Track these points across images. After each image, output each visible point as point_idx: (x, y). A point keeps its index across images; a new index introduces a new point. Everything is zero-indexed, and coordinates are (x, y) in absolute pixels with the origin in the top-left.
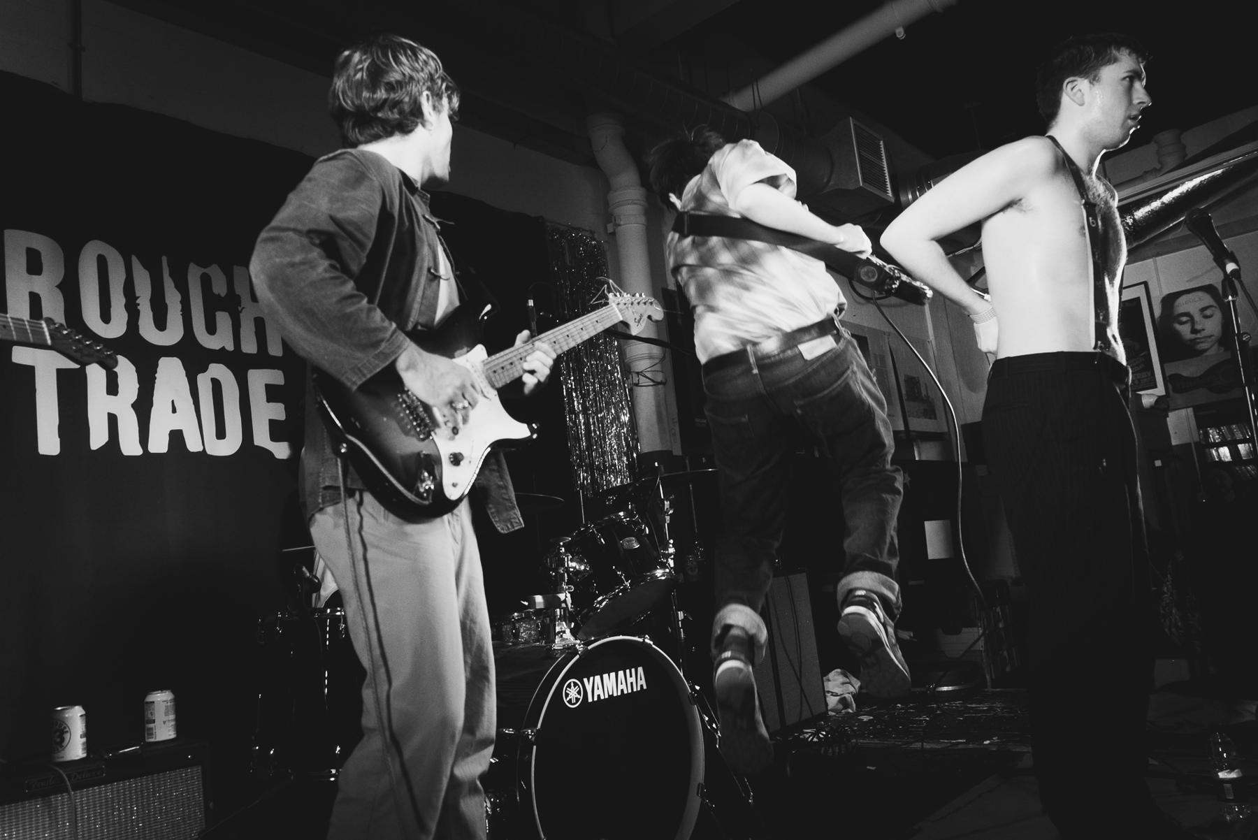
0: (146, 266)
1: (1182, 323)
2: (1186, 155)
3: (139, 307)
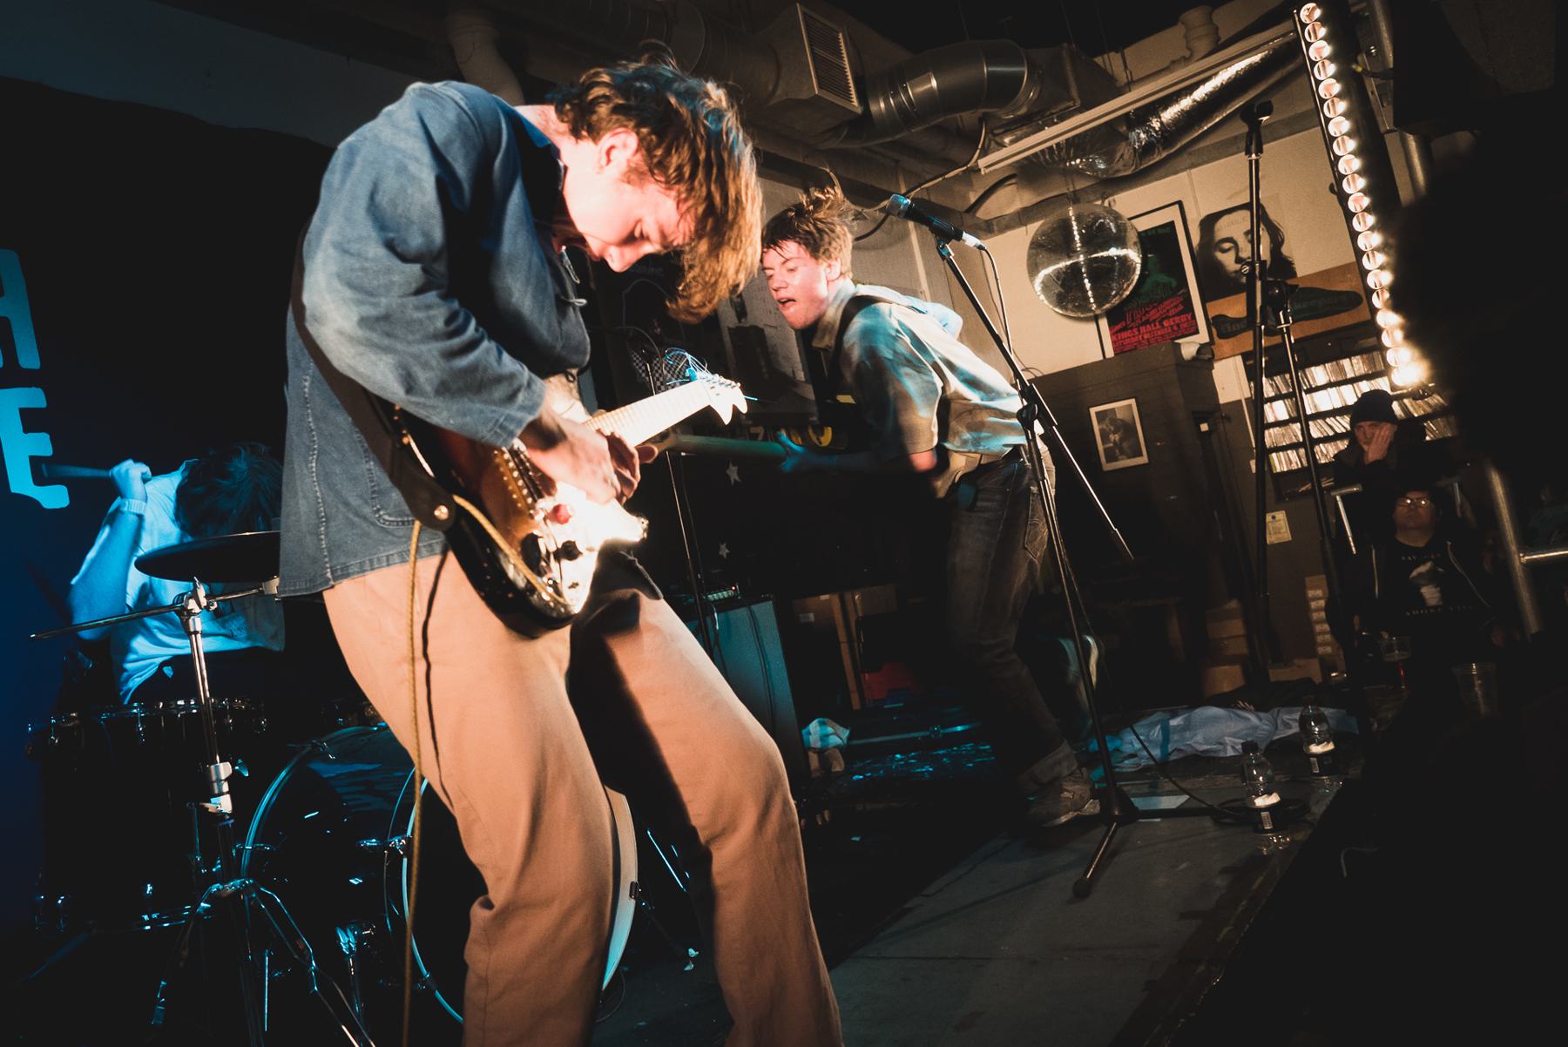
1: (1224, 251)
2: (1219, 39)
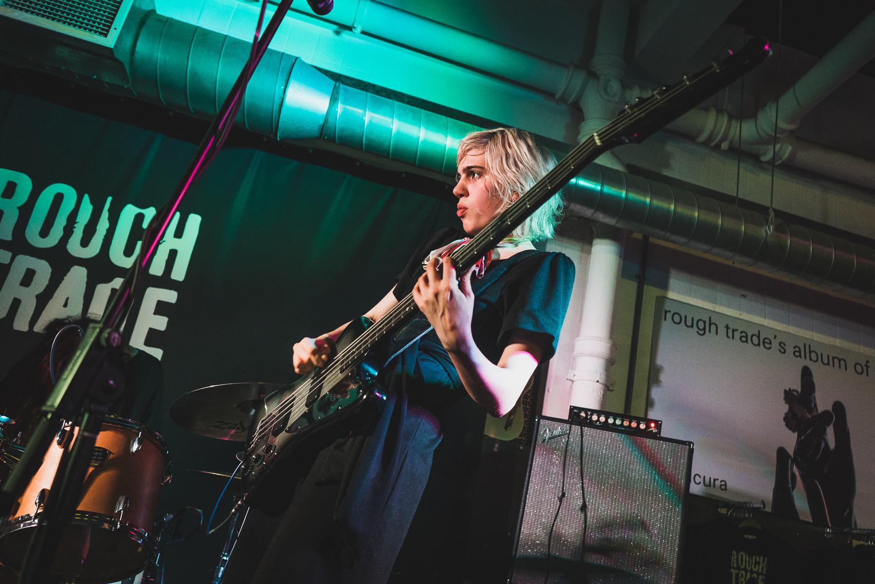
0: (92, 203)
3: (74, 230)
